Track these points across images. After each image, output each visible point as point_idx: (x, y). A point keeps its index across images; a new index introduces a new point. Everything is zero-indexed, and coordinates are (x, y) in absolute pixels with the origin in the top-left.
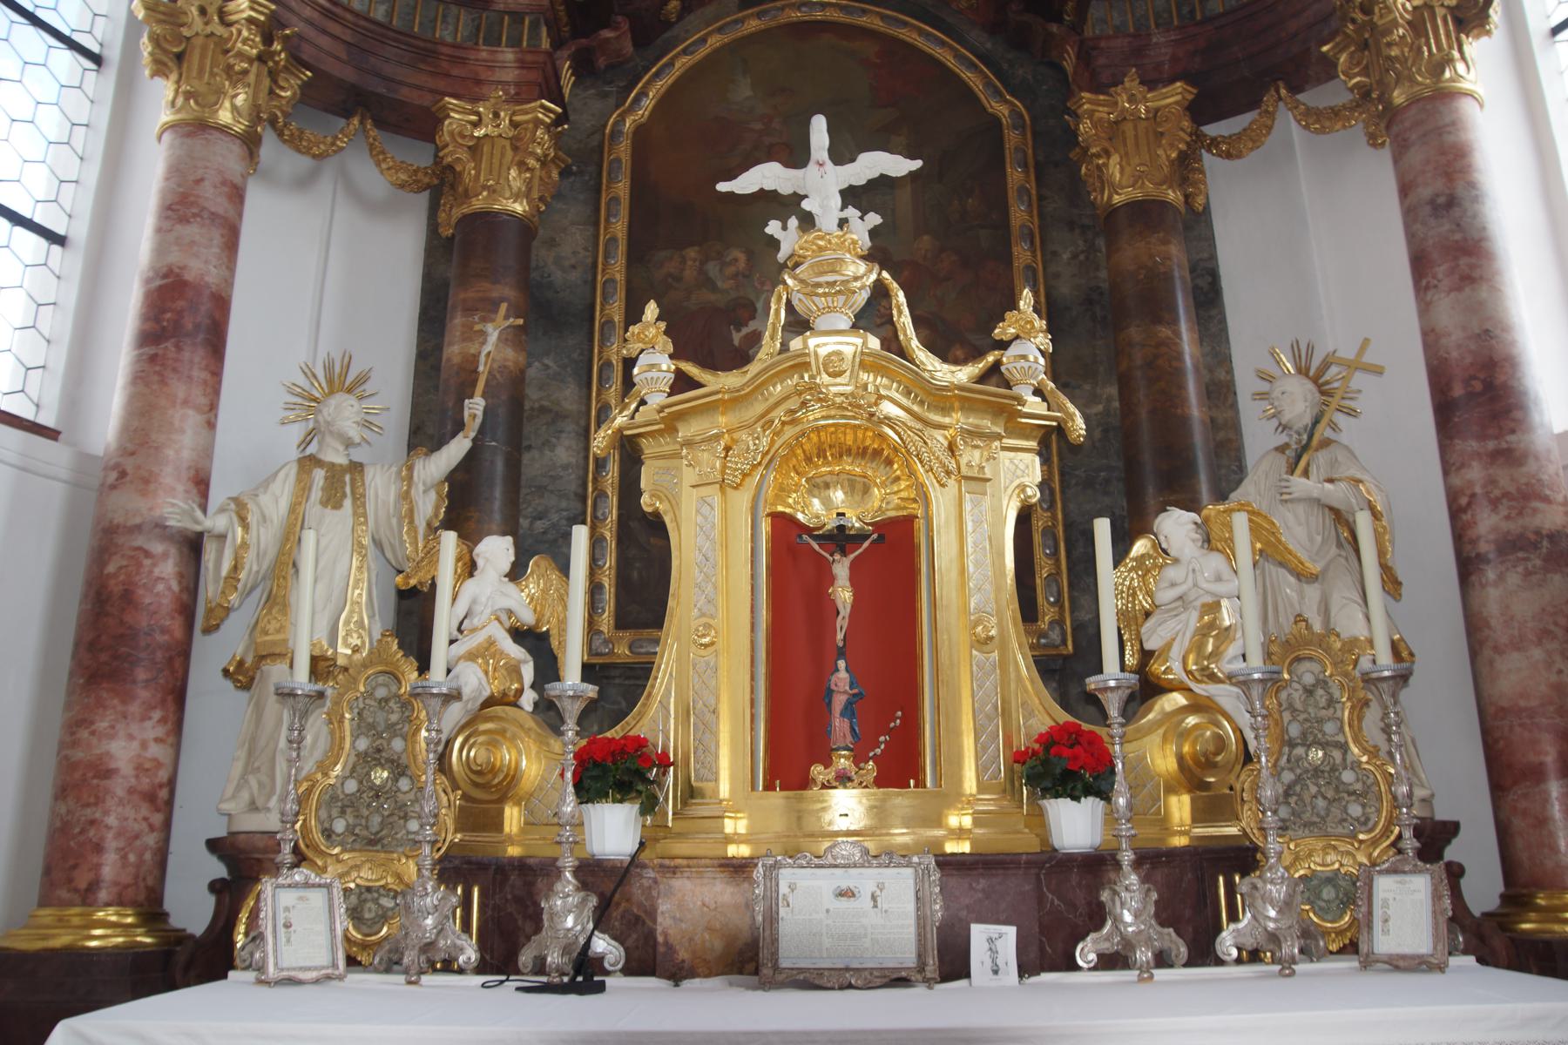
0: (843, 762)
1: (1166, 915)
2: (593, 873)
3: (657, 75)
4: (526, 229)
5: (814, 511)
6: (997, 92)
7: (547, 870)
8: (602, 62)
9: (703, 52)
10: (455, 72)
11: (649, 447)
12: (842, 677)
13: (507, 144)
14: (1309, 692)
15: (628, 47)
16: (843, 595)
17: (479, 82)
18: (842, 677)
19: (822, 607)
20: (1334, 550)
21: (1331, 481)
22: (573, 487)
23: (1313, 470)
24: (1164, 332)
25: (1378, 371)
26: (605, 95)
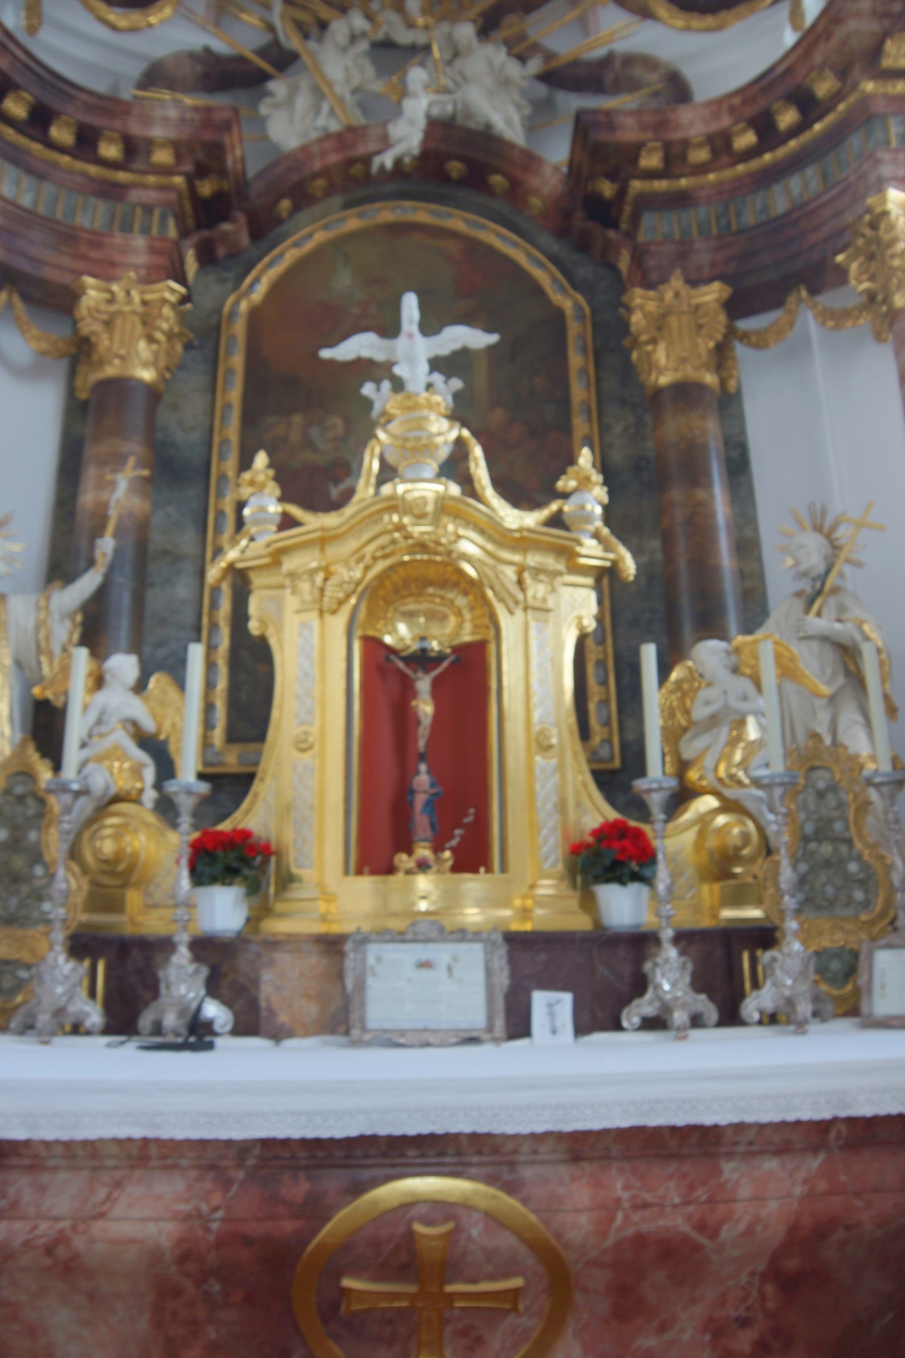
0: (423, 851)
1: (700, 983)
3: (270, 265)
4: (153, 394)
6: (562, 288)
7: (166, 945)
8: (221, 252)
9: (309, 246)
10: (94, 254)
11: (258, 580)
12: (423, 778)
13: (137, 320)
14: (821, 795)
15: (244, 239)
16: (425, 708)
17: (113, 264)
18: (423, 778)
20: (841, 680)
21: (840, 621)
23: (825, 612)
24: (701, 494)
25: (880, 528)
26: (223, 281)
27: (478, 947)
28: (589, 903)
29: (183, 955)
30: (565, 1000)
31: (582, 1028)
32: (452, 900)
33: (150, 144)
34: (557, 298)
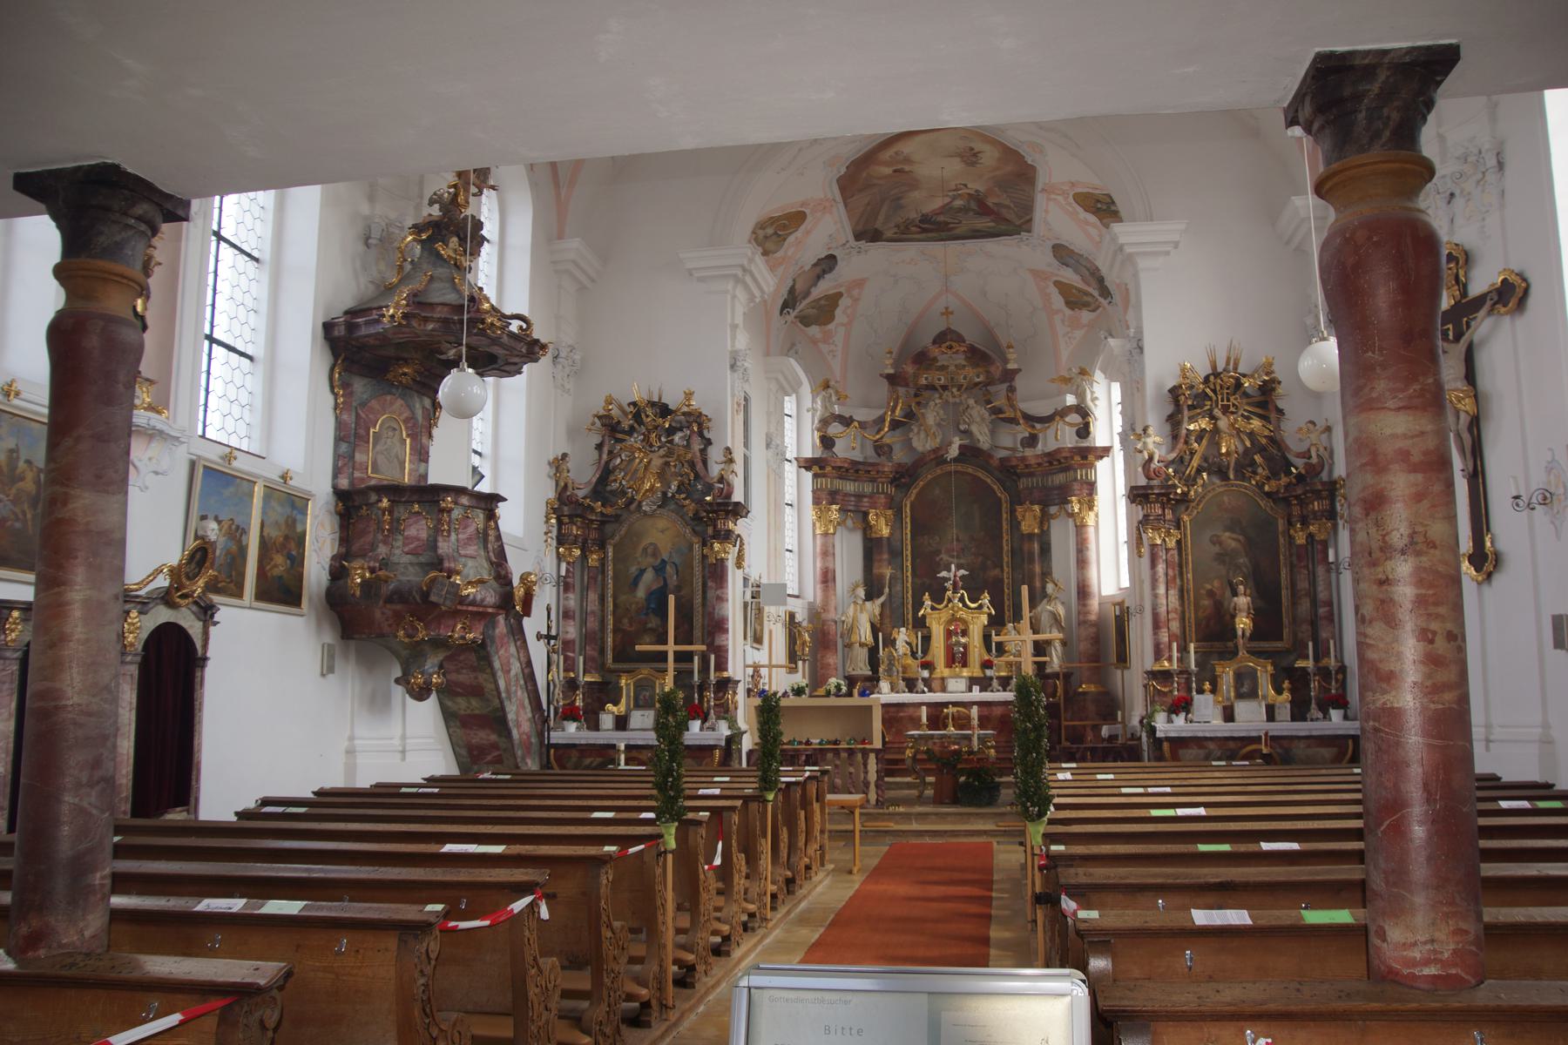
2: (924, 680)
4: (888, 538)
7: (917, 679)
22: (900, 595)
27: (964, 680)
28: (984, 673)
30: (978, 687)
31: (980, 691)
32: (961, 672)
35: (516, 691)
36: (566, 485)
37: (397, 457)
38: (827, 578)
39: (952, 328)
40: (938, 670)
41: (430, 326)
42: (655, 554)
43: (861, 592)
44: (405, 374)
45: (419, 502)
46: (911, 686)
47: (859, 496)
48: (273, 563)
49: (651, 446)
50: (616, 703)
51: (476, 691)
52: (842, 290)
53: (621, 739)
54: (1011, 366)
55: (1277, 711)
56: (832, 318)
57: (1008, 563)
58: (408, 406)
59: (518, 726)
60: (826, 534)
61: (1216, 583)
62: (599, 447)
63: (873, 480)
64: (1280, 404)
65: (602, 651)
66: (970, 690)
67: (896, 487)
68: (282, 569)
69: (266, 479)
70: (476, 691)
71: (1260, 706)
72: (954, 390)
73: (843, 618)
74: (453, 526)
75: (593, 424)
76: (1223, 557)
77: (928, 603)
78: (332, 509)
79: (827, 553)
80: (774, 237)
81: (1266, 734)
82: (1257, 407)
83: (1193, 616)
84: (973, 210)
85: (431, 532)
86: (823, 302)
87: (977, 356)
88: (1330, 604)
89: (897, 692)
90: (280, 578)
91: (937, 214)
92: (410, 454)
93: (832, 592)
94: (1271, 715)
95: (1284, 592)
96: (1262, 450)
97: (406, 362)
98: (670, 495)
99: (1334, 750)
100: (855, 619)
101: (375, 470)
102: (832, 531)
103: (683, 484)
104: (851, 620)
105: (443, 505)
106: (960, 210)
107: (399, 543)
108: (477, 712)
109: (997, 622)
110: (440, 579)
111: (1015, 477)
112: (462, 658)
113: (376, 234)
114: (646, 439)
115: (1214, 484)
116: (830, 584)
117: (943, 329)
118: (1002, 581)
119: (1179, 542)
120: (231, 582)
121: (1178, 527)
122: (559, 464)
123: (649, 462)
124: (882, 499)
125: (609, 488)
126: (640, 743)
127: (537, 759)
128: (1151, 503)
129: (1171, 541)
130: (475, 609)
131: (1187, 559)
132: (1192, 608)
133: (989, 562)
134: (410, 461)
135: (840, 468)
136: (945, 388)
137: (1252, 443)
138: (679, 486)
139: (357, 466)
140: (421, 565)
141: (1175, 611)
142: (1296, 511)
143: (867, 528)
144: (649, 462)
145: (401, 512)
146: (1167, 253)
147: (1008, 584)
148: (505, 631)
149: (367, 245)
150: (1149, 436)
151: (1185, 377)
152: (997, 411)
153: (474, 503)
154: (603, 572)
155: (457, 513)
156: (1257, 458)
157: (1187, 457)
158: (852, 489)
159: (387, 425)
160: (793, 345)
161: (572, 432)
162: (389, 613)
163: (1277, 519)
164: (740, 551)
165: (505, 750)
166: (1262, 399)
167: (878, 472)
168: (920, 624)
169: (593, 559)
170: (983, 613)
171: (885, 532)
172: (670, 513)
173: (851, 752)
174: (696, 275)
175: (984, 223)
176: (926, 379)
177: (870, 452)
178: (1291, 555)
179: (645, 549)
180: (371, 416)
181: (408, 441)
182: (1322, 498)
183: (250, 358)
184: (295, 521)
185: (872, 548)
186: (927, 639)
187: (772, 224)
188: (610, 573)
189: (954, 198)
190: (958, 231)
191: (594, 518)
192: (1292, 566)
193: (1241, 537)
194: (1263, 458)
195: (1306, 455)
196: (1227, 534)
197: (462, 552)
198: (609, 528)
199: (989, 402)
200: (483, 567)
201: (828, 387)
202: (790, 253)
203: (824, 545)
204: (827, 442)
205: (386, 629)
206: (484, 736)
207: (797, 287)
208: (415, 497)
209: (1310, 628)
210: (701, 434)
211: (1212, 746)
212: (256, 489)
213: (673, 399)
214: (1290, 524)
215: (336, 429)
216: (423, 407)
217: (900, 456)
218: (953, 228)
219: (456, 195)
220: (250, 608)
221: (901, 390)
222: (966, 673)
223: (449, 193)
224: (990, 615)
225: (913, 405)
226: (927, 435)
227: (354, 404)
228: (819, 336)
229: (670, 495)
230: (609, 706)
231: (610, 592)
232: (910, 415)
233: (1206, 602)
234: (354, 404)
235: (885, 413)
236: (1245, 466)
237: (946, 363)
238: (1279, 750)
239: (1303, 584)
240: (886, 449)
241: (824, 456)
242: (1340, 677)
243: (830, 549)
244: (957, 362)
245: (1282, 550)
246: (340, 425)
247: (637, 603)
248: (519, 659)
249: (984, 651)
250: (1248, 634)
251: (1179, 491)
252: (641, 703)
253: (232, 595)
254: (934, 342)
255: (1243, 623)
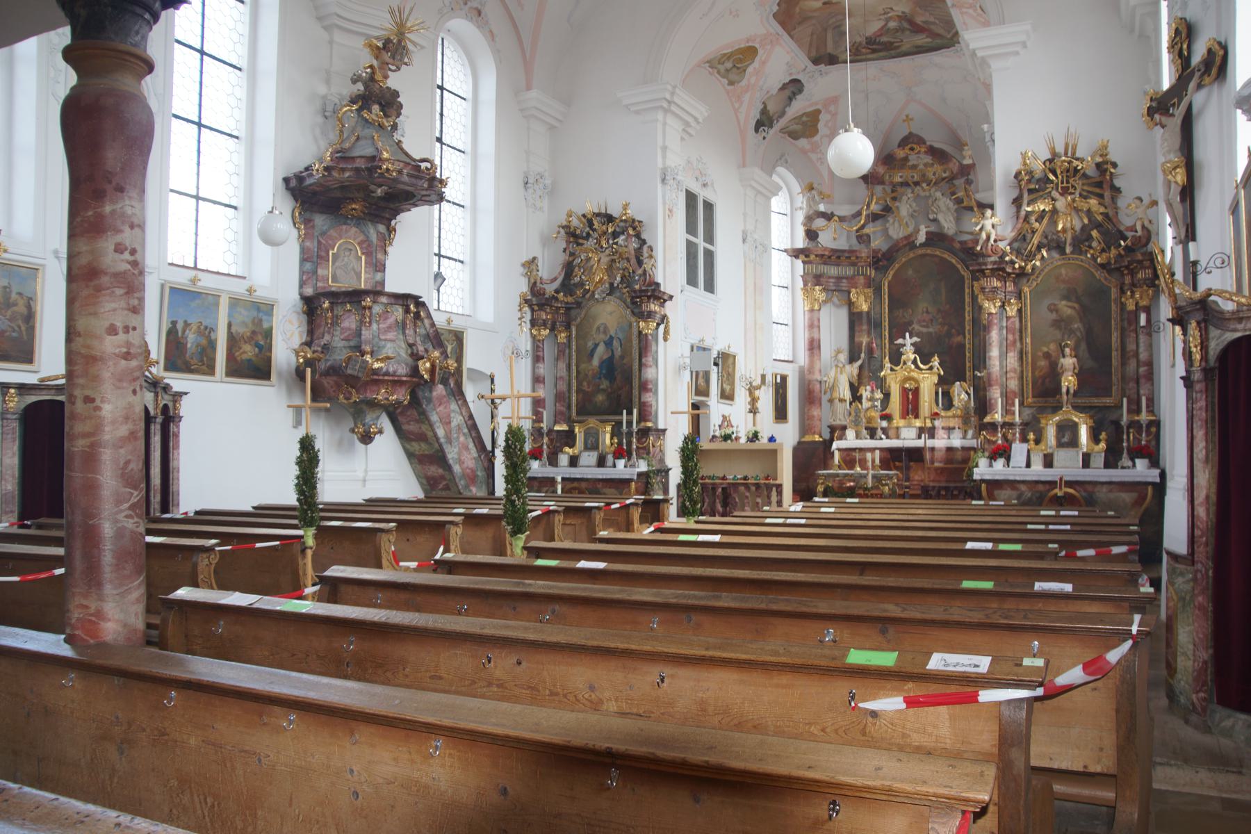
4: (868, 313)
5: (907, 386)
7: (877, 429)
12: (910, 406)
15: (885, 263)
16: (911, 397)
18: (910, 406)
19: (908, 398)
22: (880, 359)
29: (879, 430)
33: (862, 257)
34: (963, 273)
35: (458, 438)
36: (535, 283)
37: (354, 269)
38: (814, 346)
39: (914, 132)
40: (895, 421)
41: (347, 174)
42: (606, 331)
43: (843, 357)
44: (355, 209)
45: (350, 303)
46: (872, 434)
47: (839, 278)
48: (241, 351)
49: (602, 247)
50: (572, 446)
51: (422, 438)
52: (819, 107)
53: (558, 474)
54: (967, 161)
55: (1092, 459)
56: (817, 131)
57: (969, 330)
58: (363, 232)
59: (460, 462)
60: (812, 310)
61: (1052, 347)
62: (565, 250)
63: (854, 264)
64: (1117, 183)
65: (569, 407)
66: (920, 437)
67: (876, 269)
68: (250, 354)
69: (228, 292)
70: (422, 438)
71: (1078, 455)
72: (924, 185)
73: (825, 379)
74: (374, 319)
75: (559, 233)
76: (1060, 323)
77: (888, 365)
78: (299, 310)
79: (813, 325)
80: (735, 70)
81: (1061, 479)
82: (1095, 187)
83: (1030, 375)
84: (909, 30)
85: (358, 324)
86: (804, 119)
87: (939, 155)
88: (1150, 364)
89: (861, 439)
90: (249, 361)
91: (878, 36)
92: (366, 267)
93: (816, 357)
94: (1086, 462)
95: (1115, 355)
96: (1098, 226)
97: (353, 200)
98: (616, 285)
99: (1135, 495)
100: (836, 380)
101: (335, 279)
102: (816, 307)
103: (625, 276)
104: (832, 380)
105: (363, 303)
106: (896, 30)
107: (338, 333)
108: (426, 452)
109: (942, 381)
110: (354, 357)
111: (974, 258)
112: (409, 413)
113: (330, 108)
114: (599, 242)
115: (1053, 258)
116: (816, 351)
117: (906, 133)
118: (964, 346)
119: (1020, 311)
120: (204, 364)
121: (1020, 298)
122: (531, 264)
123: (599, 261)
124: (861, 280)
125: (572, 282)
126: (578, 476)
127: (484, 487)
128: (987, 277)
129: (1012, 310)
130: (391, 378)
131: (1026, 325)
132: (1030, 369)
133: (953, 330)
134: (366, 272)
135: (822, 256)
136: (917, 184)
137: (1090, 220)
138: (622, 278)
139: (320, 278)
140: (350, 347)
141: (1014, 371)
142: (1128, 280)
143: (850, 304)
144: (599, 261)
145: (339, 310)
146: (1017, 53)
147: (969, 348)
148: (444, 393)
149: (326, 117)
150: (987, 219)
151: (1025, 164)
152: (959, 201)
153: (393, 301)
154: (569, 347)
155: (377, 309)
156: (1095, 233)
157: (1029, 236)
158: (836, 273)
159: (344, 247)
160: (782, 155)
161: (545, 241)
162: (332, 382)
163: (1110, 288)
164: (666, 328)
165: (450, 480)
166: (1098, 180)
167: (857, 258)
168: (881, 384)
169: (562, 337)
170: (934, 373)
171: (865, 307)
172: (616, 300)
173: (758, 486)
174: (634, 108)
175: (921, 40)
176: (901, 177)
177: (854, 241)
178: (1122, 320)
179: (598, 328)
180: (330, 242)
181: (363, 257)
182: (1145, 268)
183: (235, 208)
184: (261, 320)
185: (855, 319)
186: (887, 396)
187: (729, 58)
188: (574, 347)
189: (887, 20)
190: (904, 48)
191: (559, 305)
192: (1123, 332)
193: (1076, 306)
194: (1098, 232)
195: (1133, 229)
196: (1064, 303)
197: (383, 337)
198: (573, 313)
199: (953, 194)
200: (400, 347)
201: (813, 189)
202: (753, 80)
203: (811, 320)
204: (811, 235)
205: (333, 394)
206: (435, 470)
207: (769, 108)
208: (347, 299)
209: (1135, 385)
210: (638, 236)
211: (1023, 488)
212: (221, 300)
213: (615, 211)
214: (1123, 292)
215: (300, 254)
216: (378, 232)
217: (878, 243)
218: (899, 47)
219: (373, 73)
220: (221, 382)
221: (878, 189)
222: (918, 423)
223: (366, 73)
224: (939, 375)
225: (888, 199)
226: (900, 225)
227: (316, 234)
228: (808, 147)
229: (616, 285)
230: (567, 449)
231: (574, 361)
232: (887, 209)
233: (1043, 363)
234: (316, 234)
235: (862, 208)
236: (1081, 241)
237: (915, 163)
238: (1084, 494)
239: (1131, 347)
240: (865, 238)
241: (810, 246)
242: (1153, 429)
243: (816, 323)
244: (925, 161)
245: (1114, 315)
246: (303, 250)
247: (593, 370)
248: (461, 414)
249: (934, 405)
250: (1072, 391)
251: (1017, 266)
252: (589, 446)
253: (204, 374)
254: (899, 146)
255: (1069, 381)
